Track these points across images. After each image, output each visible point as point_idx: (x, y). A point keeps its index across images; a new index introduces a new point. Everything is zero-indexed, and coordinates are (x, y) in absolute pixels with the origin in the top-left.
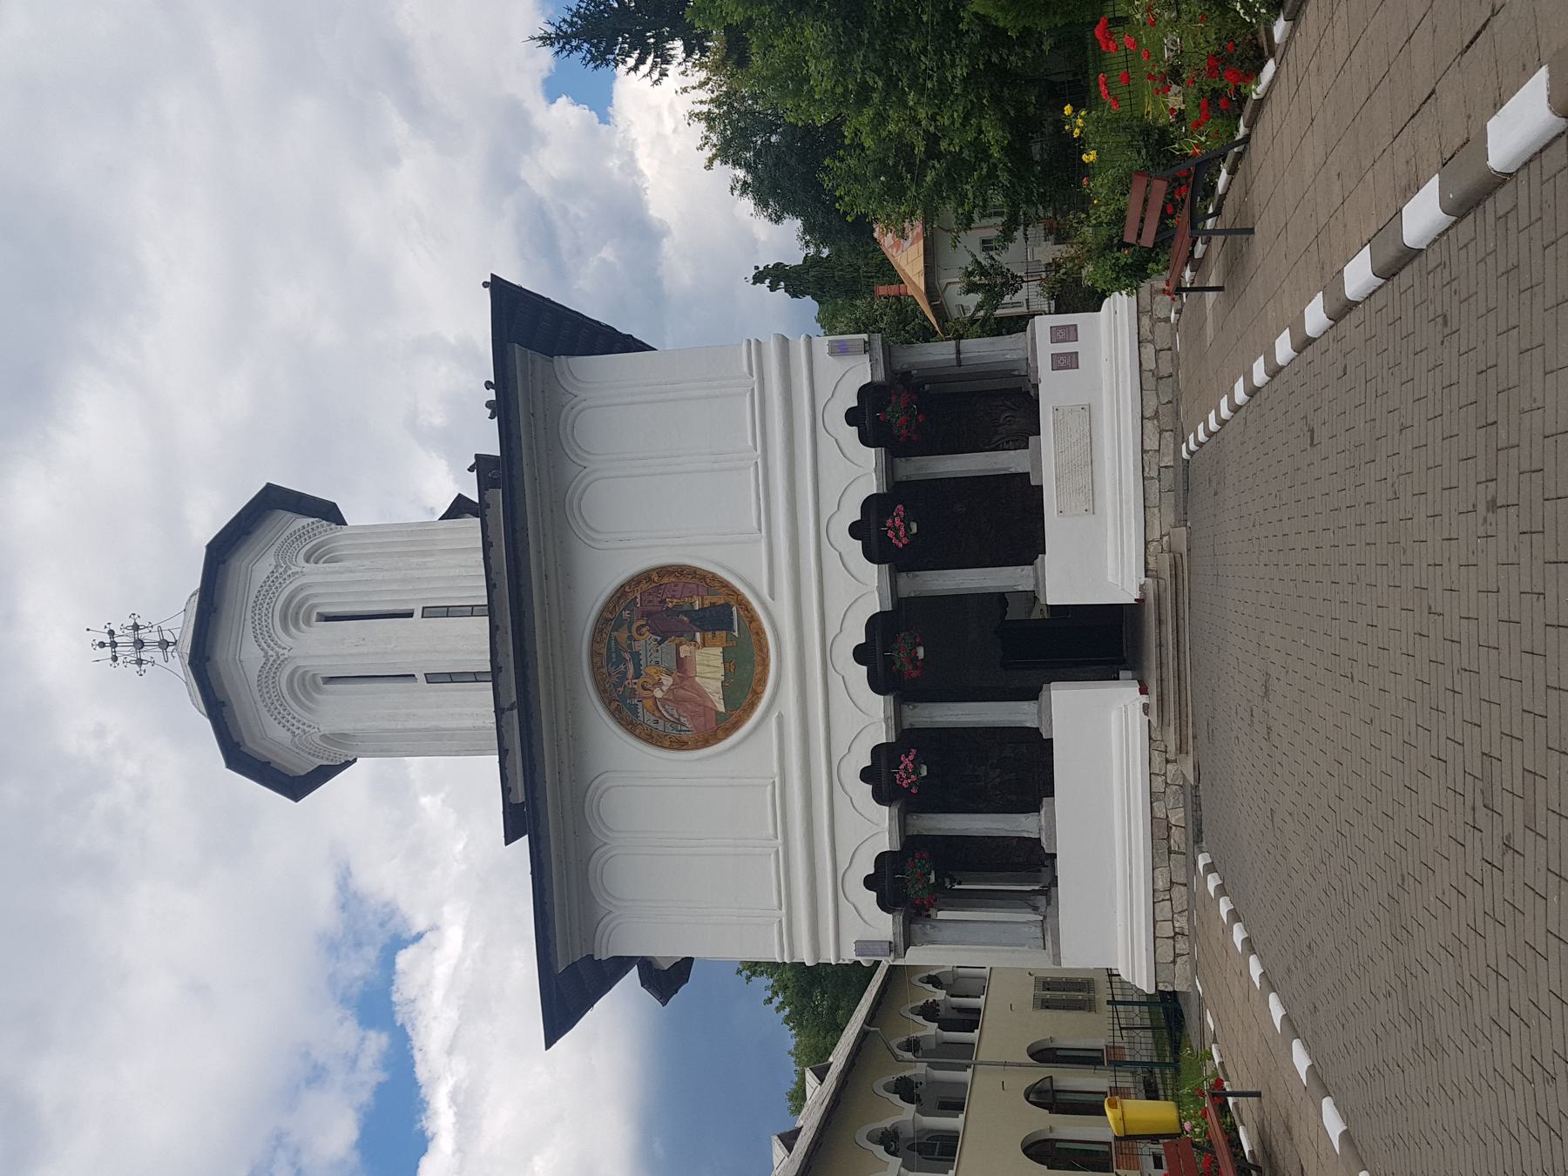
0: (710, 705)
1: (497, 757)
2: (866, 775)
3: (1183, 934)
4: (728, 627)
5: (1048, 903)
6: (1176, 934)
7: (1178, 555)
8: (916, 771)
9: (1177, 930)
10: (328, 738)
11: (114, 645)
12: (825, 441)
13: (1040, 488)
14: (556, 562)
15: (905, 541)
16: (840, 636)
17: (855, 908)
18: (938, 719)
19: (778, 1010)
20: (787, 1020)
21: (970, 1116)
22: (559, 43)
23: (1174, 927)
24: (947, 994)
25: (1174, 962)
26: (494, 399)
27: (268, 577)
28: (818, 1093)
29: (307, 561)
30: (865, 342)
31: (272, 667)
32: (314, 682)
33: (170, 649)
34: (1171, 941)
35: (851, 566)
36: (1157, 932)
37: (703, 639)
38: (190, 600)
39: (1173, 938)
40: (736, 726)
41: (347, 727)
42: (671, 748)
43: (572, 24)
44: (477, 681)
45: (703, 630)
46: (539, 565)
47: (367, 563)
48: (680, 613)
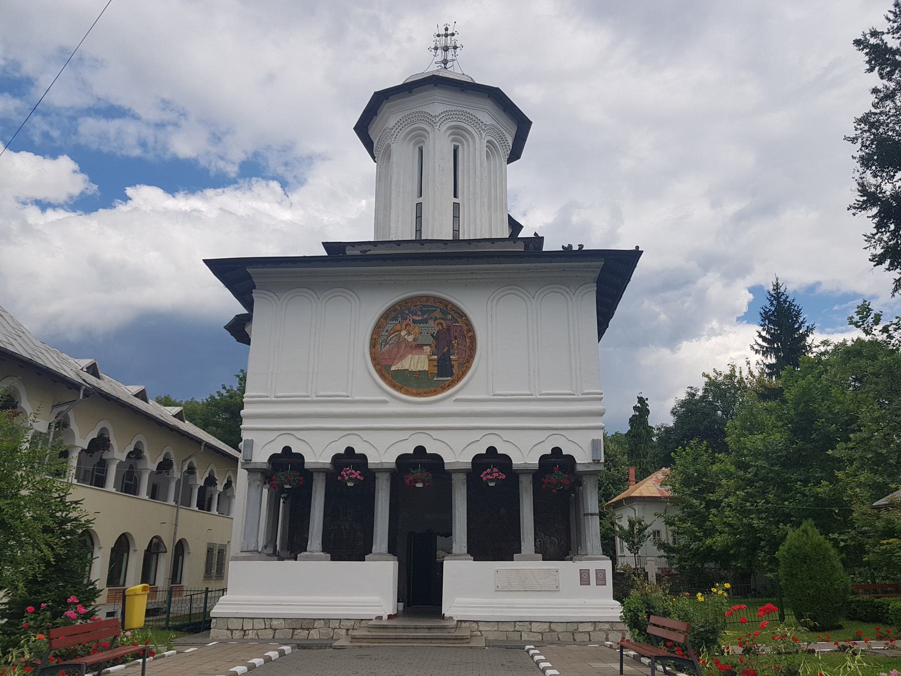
0: (395, 362)
1: (373, 240)
2: (350, 450)
3: (244, 635)
4: (440, 375)
5: (268, 555)
7: (468, 641)
8: (350, 479)
9: (247, 632)
10: (389, 148)
11: (446, 36)
12: (544, 435)
14: (481, 279)
15: (484, 479)
16: (431, 439)
17: (274, 440)
18: (380, 494)
19: (218, 392)
20: (212, 397)
21: (147, 502)
22: (775, 294)
23: (249, 630)
24: (221, 492)
25: (228, 629)
26: (573, 249)
27: (480, 120)
28: (167, 414)
29: (487, 141)
30: (599, 460)
31: (430, 119)
32: (420, 142)
33: (443, 65)
35: (471, 447)
36: (247, 619)
37: (433, 360)
38: (469, 77)
39: (242, 629)
40: (382, 376)
41: (394, 158)
42: (372, 338)
43: (785, 301)
44: (416, 231)
45: (438, 360)
46: (479, 270)
47: (486, 174)
48: (449, 347)
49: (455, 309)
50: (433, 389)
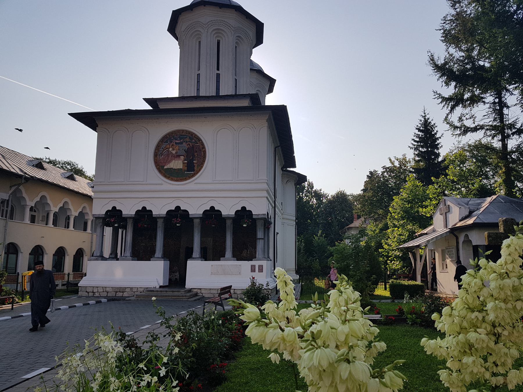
3: (94, 295)
6: (94, 293)
13: (220, 260)
25: (86, 292)
34: (92, 291)
37: (185, 163)
39: (93, 292)
42: (155, 152)
45: (187, 163)
49: (196, 137)
50: (184, 178)
